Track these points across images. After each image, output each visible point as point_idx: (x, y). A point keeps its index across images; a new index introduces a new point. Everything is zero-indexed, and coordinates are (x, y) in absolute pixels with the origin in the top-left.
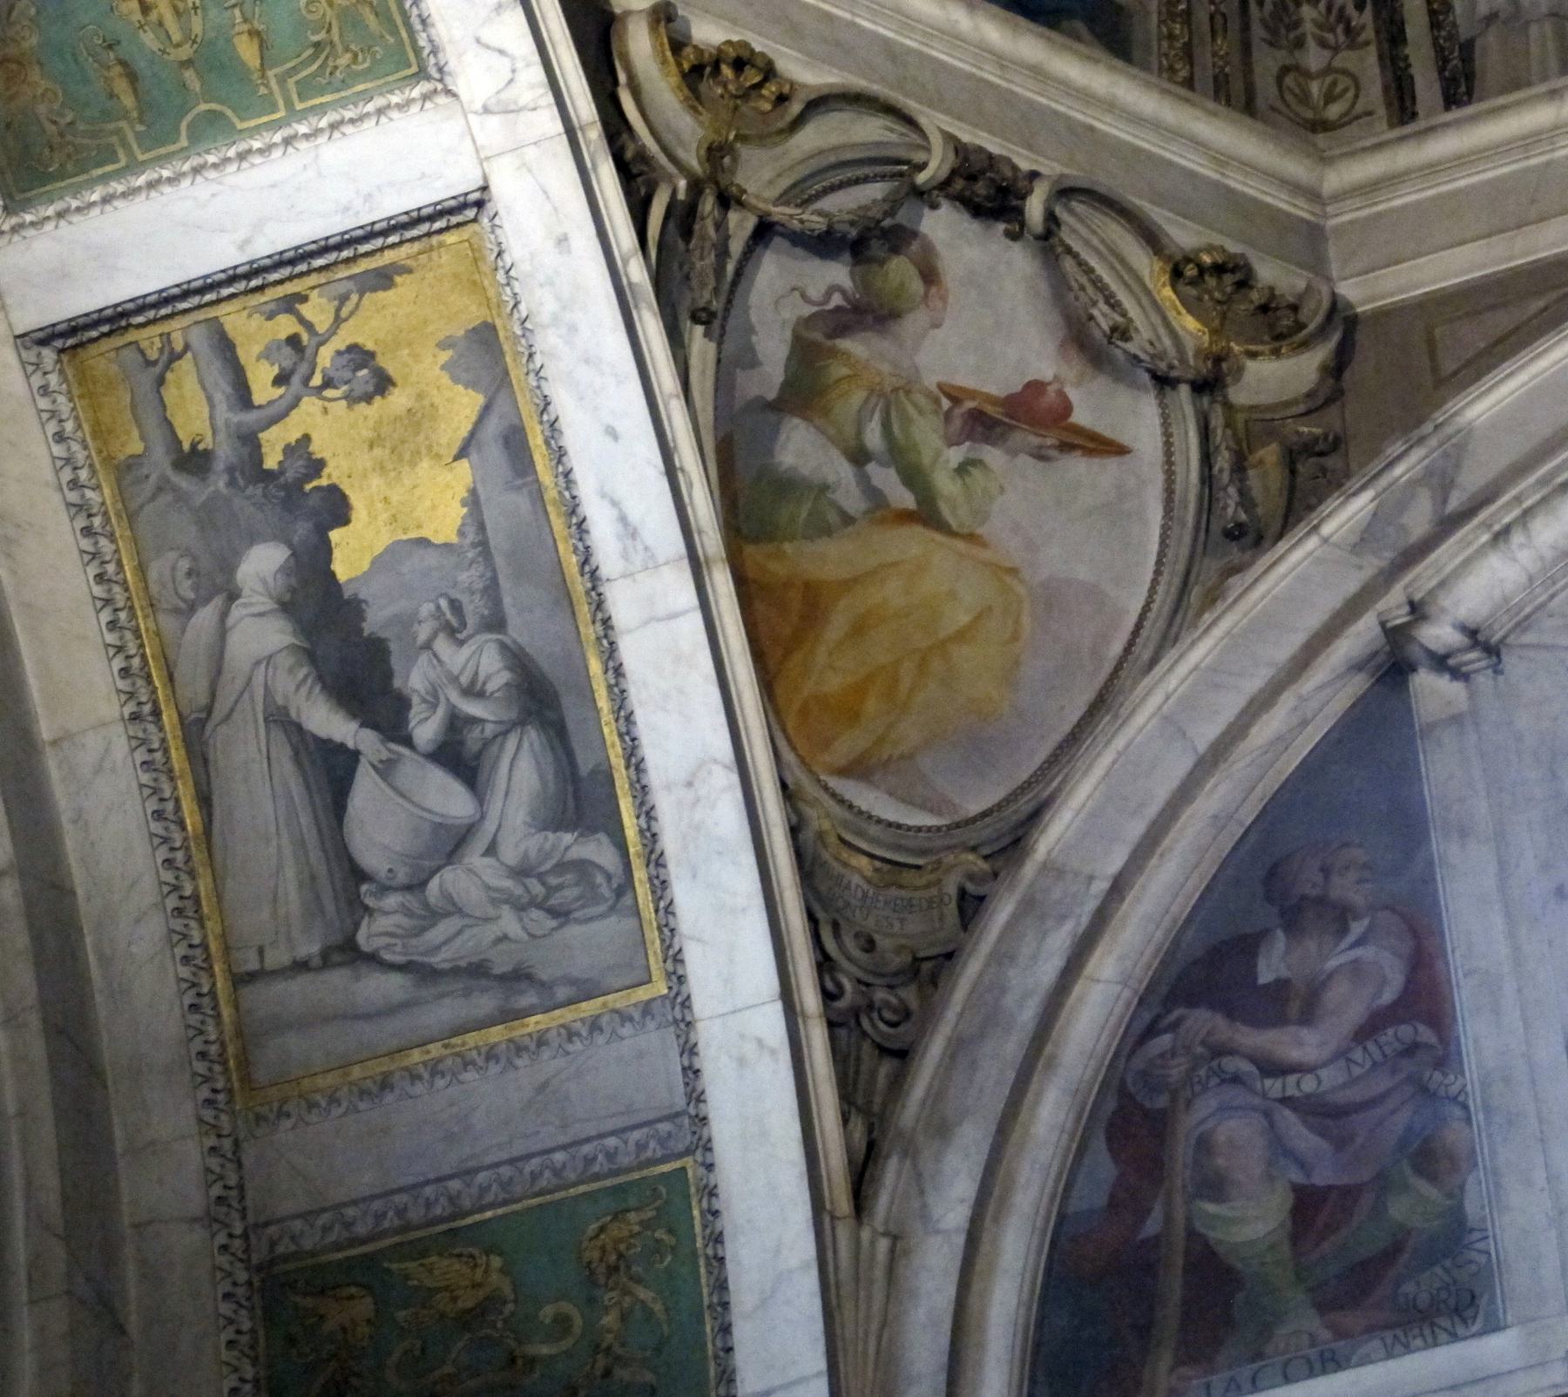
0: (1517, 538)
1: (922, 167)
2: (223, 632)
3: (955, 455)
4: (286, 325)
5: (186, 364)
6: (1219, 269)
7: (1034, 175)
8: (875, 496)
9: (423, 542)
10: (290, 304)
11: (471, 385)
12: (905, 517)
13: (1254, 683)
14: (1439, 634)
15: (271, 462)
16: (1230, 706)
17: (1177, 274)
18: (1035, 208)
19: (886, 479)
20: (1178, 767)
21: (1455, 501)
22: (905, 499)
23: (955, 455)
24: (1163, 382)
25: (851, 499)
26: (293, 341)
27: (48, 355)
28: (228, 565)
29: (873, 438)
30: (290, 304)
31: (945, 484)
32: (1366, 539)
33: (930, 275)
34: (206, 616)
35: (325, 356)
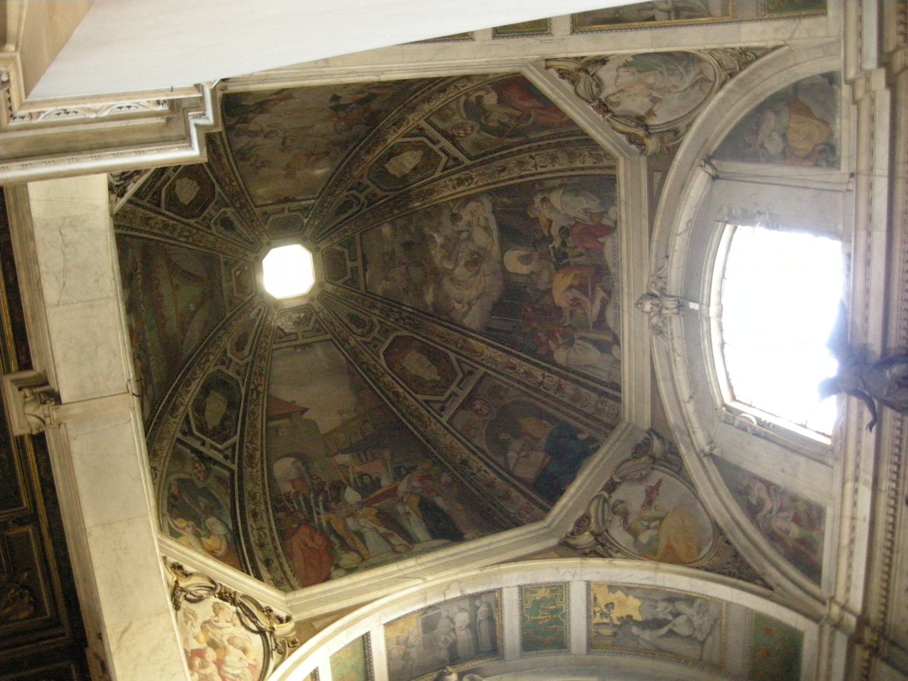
0: (695, 430)
1: (604, 498)
2: (644, 640)
3: (653, 510)
4: (598, 614)
5: (599, 630)
6: (636, 449)
7: (611, 478)
8: (656, 528)
9: (640, 607)
10: (595, 613)
11: (616, 591)
12: (660, 523)
13: (706, 479)
14: (707, 449)
15: (618, 623)
16: (708, 484)
17: (635, 458)
18: (617, 480)
19: (653, 524)
20: (715, 497)
21: (686, 432)
22: (657, 522)
23: (653, 510)
24: (653, 468)
25: (654, 532)
26: (601, 614)
27: (592, 650)
28: (634, 635)
29: (646, 523)
30: (595, 613)
31: (657, 514)
32: (687, 448)
33: (622, 502)
34: (641, 642)
35: (605, 610)
